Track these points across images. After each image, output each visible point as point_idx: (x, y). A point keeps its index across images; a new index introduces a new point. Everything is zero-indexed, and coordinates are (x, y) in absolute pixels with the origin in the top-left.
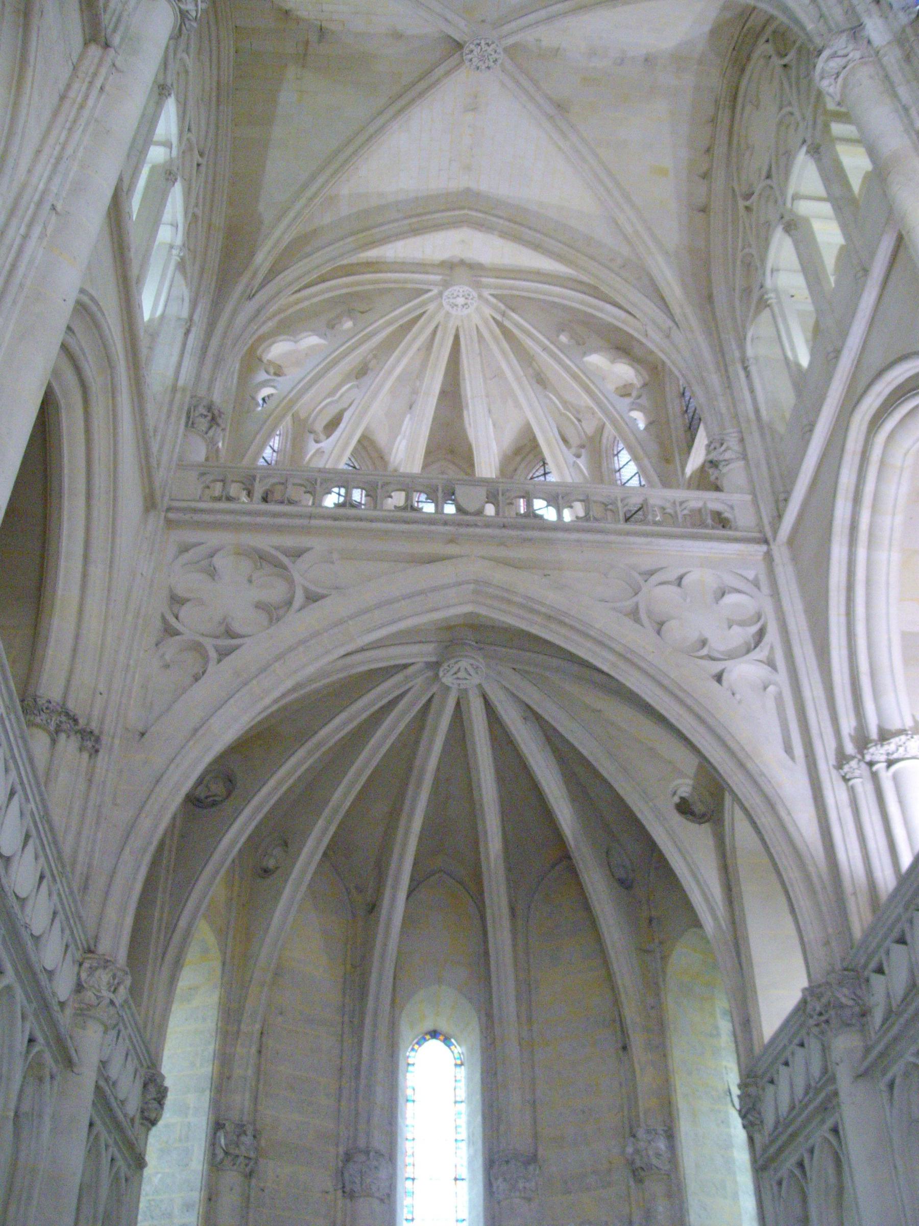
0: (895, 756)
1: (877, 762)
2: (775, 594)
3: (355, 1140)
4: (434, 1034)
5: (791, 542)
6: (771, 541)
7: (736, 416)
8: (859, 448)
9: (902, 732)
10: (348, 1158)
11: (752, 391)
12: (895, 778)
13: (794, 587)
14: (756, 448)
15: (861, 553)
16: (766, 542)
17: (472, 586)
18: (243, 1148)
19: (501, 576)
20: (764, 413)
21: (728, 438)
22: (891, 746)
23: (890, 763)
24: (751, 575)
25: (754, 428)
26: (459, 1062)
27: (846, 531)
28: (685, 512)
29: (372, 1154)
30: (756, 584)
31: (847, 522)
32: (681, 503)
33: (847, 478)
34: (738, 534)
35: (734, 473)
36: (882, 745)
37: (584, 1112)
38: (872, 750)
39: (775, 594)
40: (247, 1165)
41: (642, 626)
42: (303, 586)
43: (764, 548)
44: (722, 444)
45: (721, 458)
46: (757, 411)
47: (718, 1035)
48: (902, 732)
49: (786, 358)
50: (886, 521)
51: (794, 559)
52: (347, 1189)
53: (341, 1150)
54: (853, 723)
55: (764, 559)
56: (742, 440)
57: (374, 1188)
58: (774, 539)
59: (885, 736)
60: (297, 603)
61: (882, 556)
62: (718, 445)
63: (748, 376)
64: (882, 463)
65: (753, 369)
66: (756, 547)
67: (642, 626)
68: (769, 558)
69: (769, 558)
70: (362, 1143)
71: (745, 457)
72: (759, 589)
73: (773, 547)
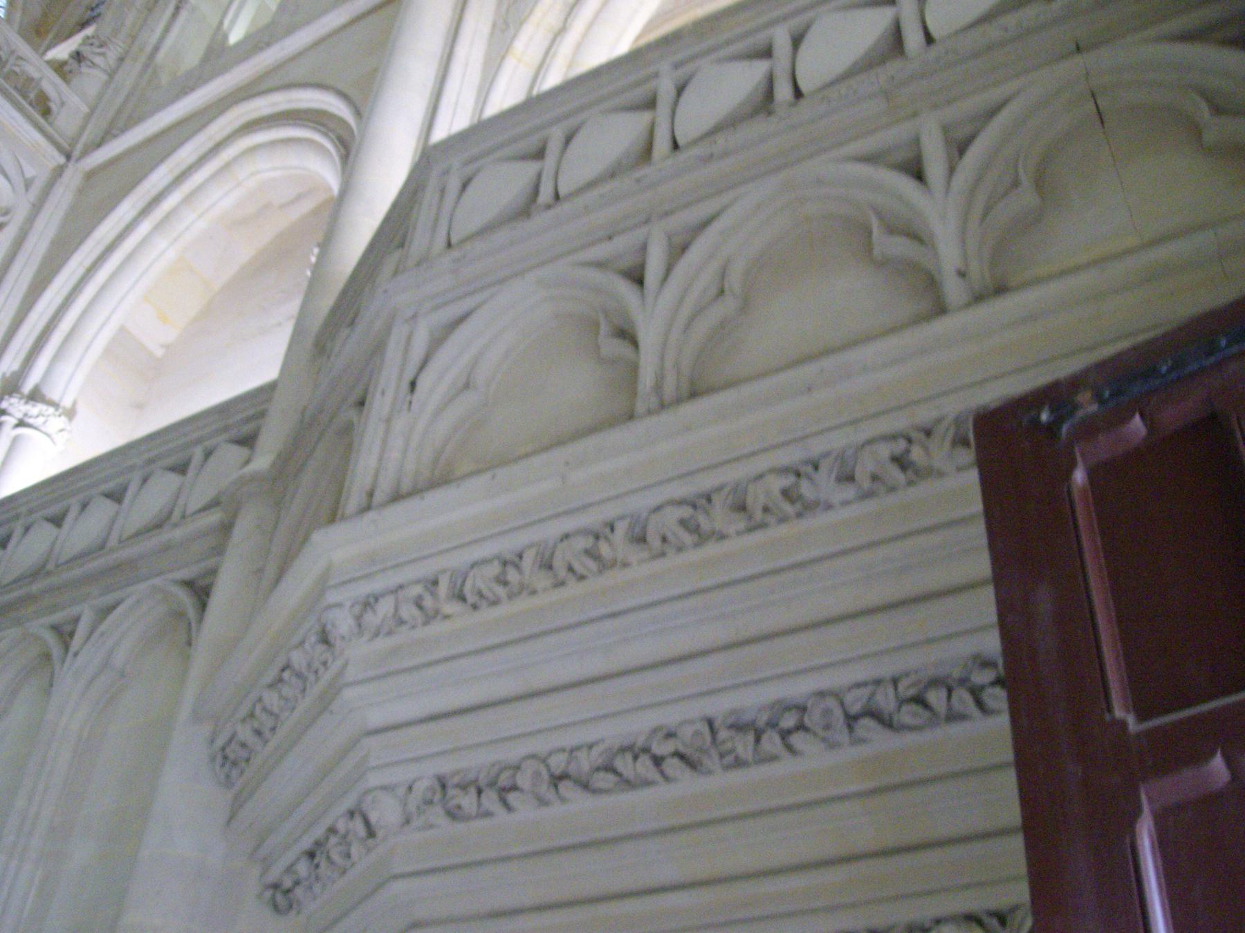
0: (31, 421)
1: (9, 414)
2: (37, 208)
5: (90, 175)
6: (74, 158)
7: (134, 38)
8: (218, 138)
9: (55, 405)
11: (167, 29)
12: (15, 440)
13: (60, 213)
14: (128, 77)
15: (145, 227)
16: (68, 157)
20: (161, 56)
21: (111, 47)
22: (35, 409)
23: (21, 424)
24: (30, 172)
25: (143, 59)
27: (148, 198)
28: (17, 69)
30: (28, 184)
31: (154, 192)
32: (20, 58)
33: (187, 153)
34: (49, 129)
35: (91, 80)
36: (26, 403)
38: (14, 400)
39: (37, 208)
43: (62, 160)
44: (101, 46)
45: (90, 57)
46: (156, 49)
48: (55, 405)
49: (221, 23)
50: (189, 217)
51: (81, 191)
54: (16, 366)
55: (54, 170)
56: (121, 60)
58: (78, 159)
59: (36, 396)
61: (161, 243)
62: (97, 43)
63: (175, 15)
64: (227, 166)
65: (184, 14)
66: (56, 153)
68: (59, 172)
69: (59, 172)
71: (111, 74)
72: (27, 190)
73: (70, 165)
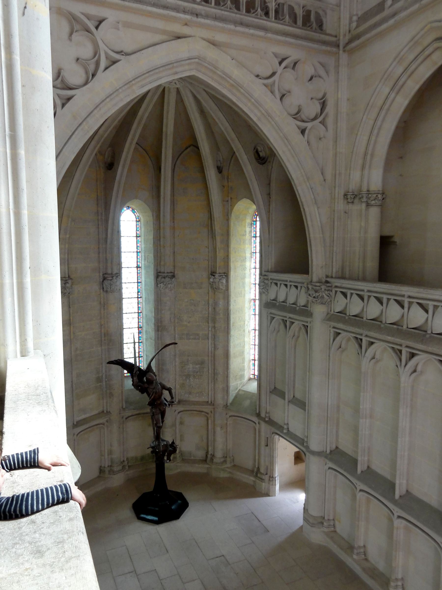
3: (106, 269)
10: (104, 279)
17: (197, 60)
18: (67, 289)
19: (212, 54)
26: (138, 220)
37: (193, 259)
41: (275, 97)
42: (105, 51)
47: (246, 235)
52: (105, 289)
53: (101, 274)
57: (115, 289)
60: (103, 65)
67: (275, 97)
70: (109, 271)
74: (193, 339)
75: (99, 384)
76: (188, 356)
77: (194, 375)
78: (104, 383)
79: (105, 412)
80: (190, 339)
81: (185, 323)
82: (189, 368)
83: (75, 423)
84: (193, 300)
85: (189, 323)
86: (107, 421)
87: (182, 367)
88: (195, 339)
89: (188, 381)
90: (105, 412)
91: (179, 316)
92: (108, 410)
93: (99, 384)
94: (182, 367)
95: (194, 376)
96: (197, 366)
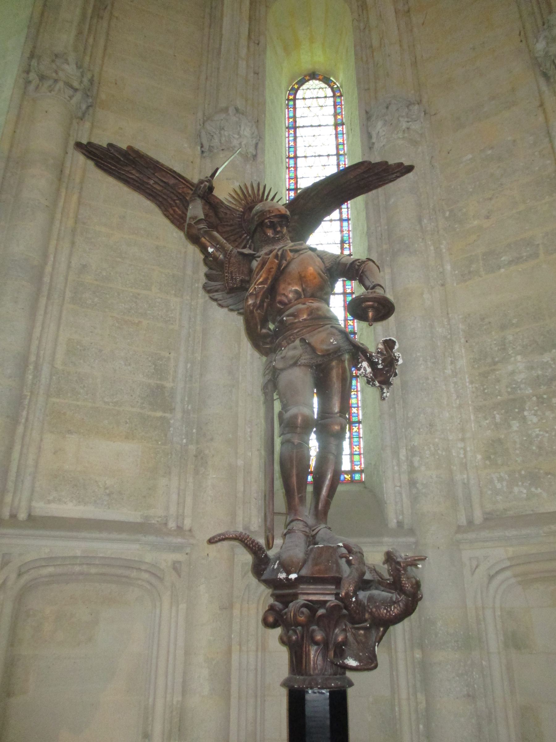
4: (313, 76)
29: (231, 111)
40: (71, 97)
52: (206, 147)
74: (510, 263)
75: (159, 414)
76: (503, 327)
77: (539, 397)
78: (179, 415)
79: (172, 525)
80: (499, 268)
81: (476, 223)
82: (513, 373)
83: (22, 516)
84: (492, 148)
85: (488, 217)
86: (176, 567)
87: (485, 375)
88: (517, 261)
89: (515, 425)
90: (172, 525)
91: (451, 211)
92: (187, 523)
93: (159, 414)
94: (485, 375)
95: (541, 401)
96: (547, 358)
